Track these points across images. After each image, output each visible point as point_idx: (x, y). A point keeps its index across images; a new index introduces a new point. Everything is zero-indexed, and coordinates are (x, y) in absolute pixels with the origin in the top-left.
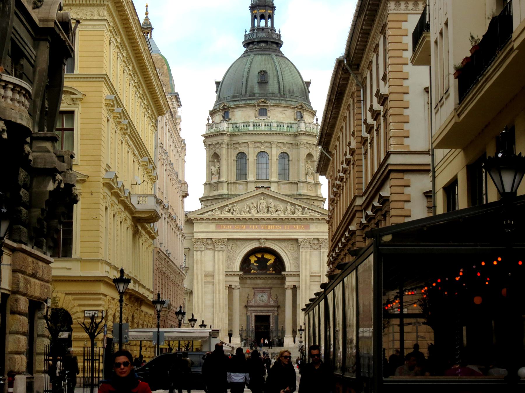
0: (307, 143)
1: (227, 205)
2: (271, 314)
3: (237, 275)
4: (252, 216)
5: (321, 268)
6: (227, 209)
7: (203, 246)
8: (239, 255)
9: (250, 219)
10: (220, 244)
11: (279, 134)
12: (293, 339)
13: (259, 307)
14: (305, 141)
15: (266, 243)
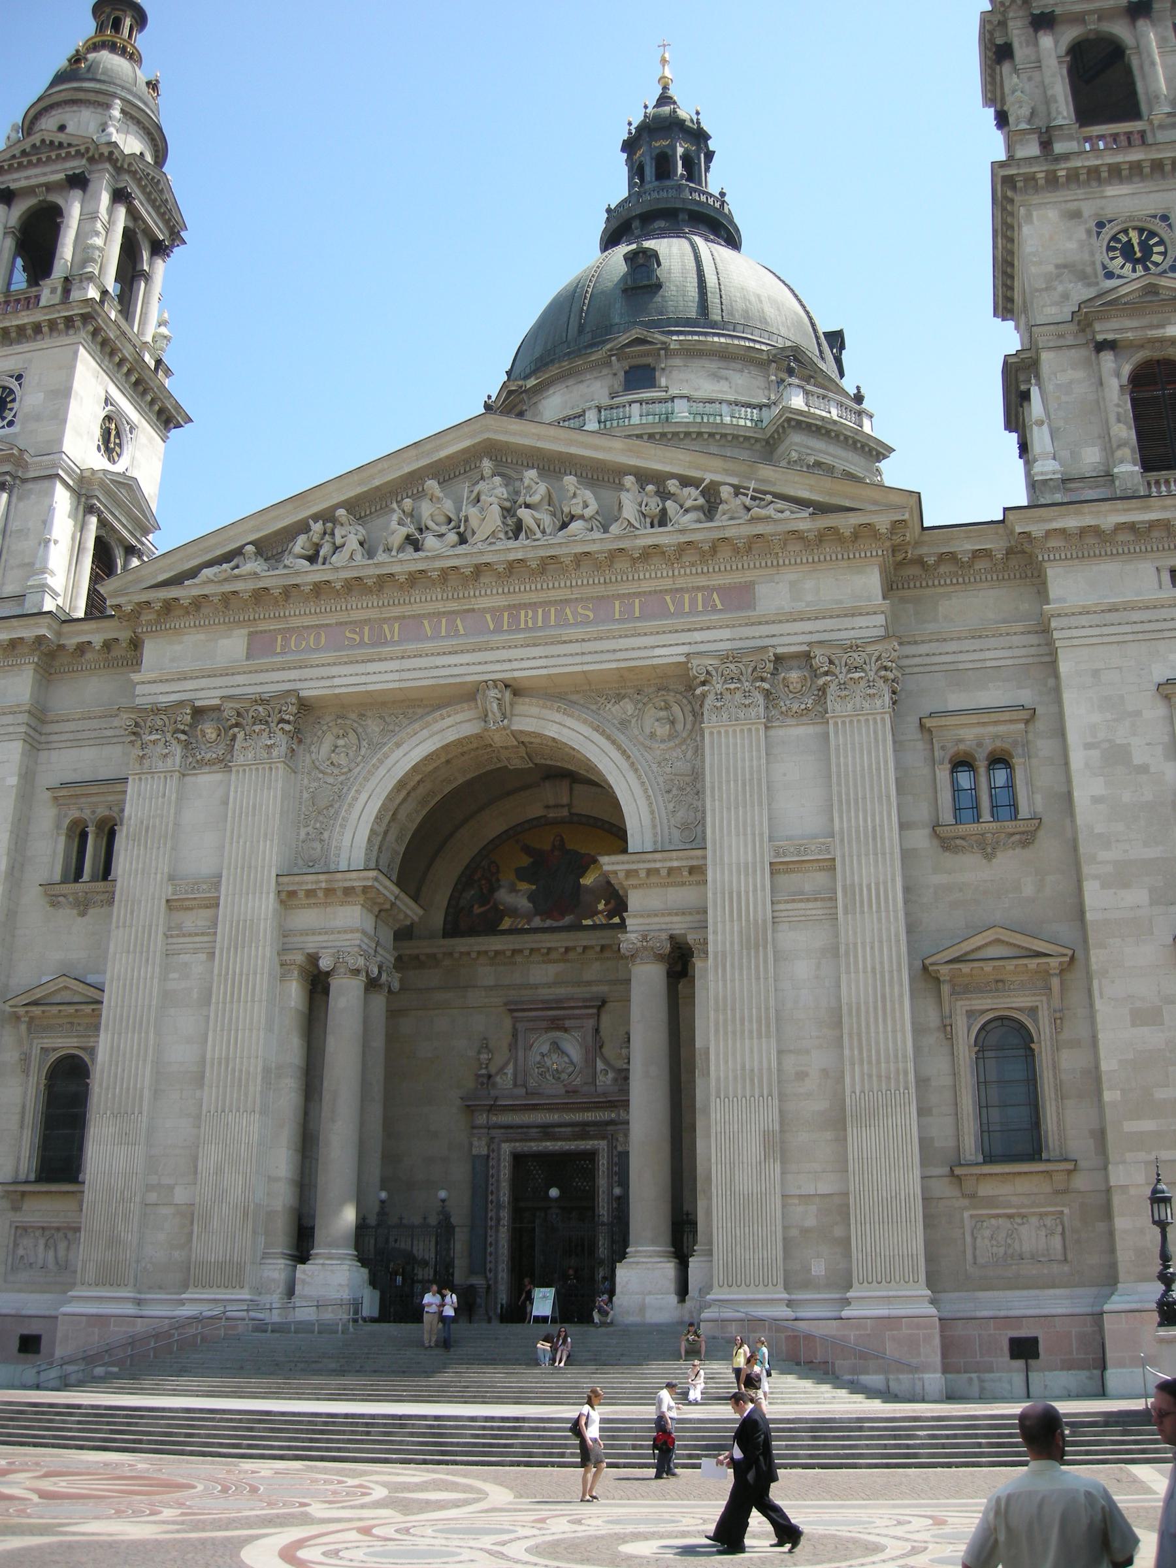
0: (818, 464)
1: (303, 527)
2: (602, 1145)
3: (348, 891)
4: (427, 557)
5: (832, 820)
6: (300, 544)
7: (178, 750)
8: (370, 785)
9: (415, 579)
10: (257, 728)
11: (700, 434)
12: (669, 1269)
13: (534, 1107)
14: (809, 451)
15: (519, 709)
